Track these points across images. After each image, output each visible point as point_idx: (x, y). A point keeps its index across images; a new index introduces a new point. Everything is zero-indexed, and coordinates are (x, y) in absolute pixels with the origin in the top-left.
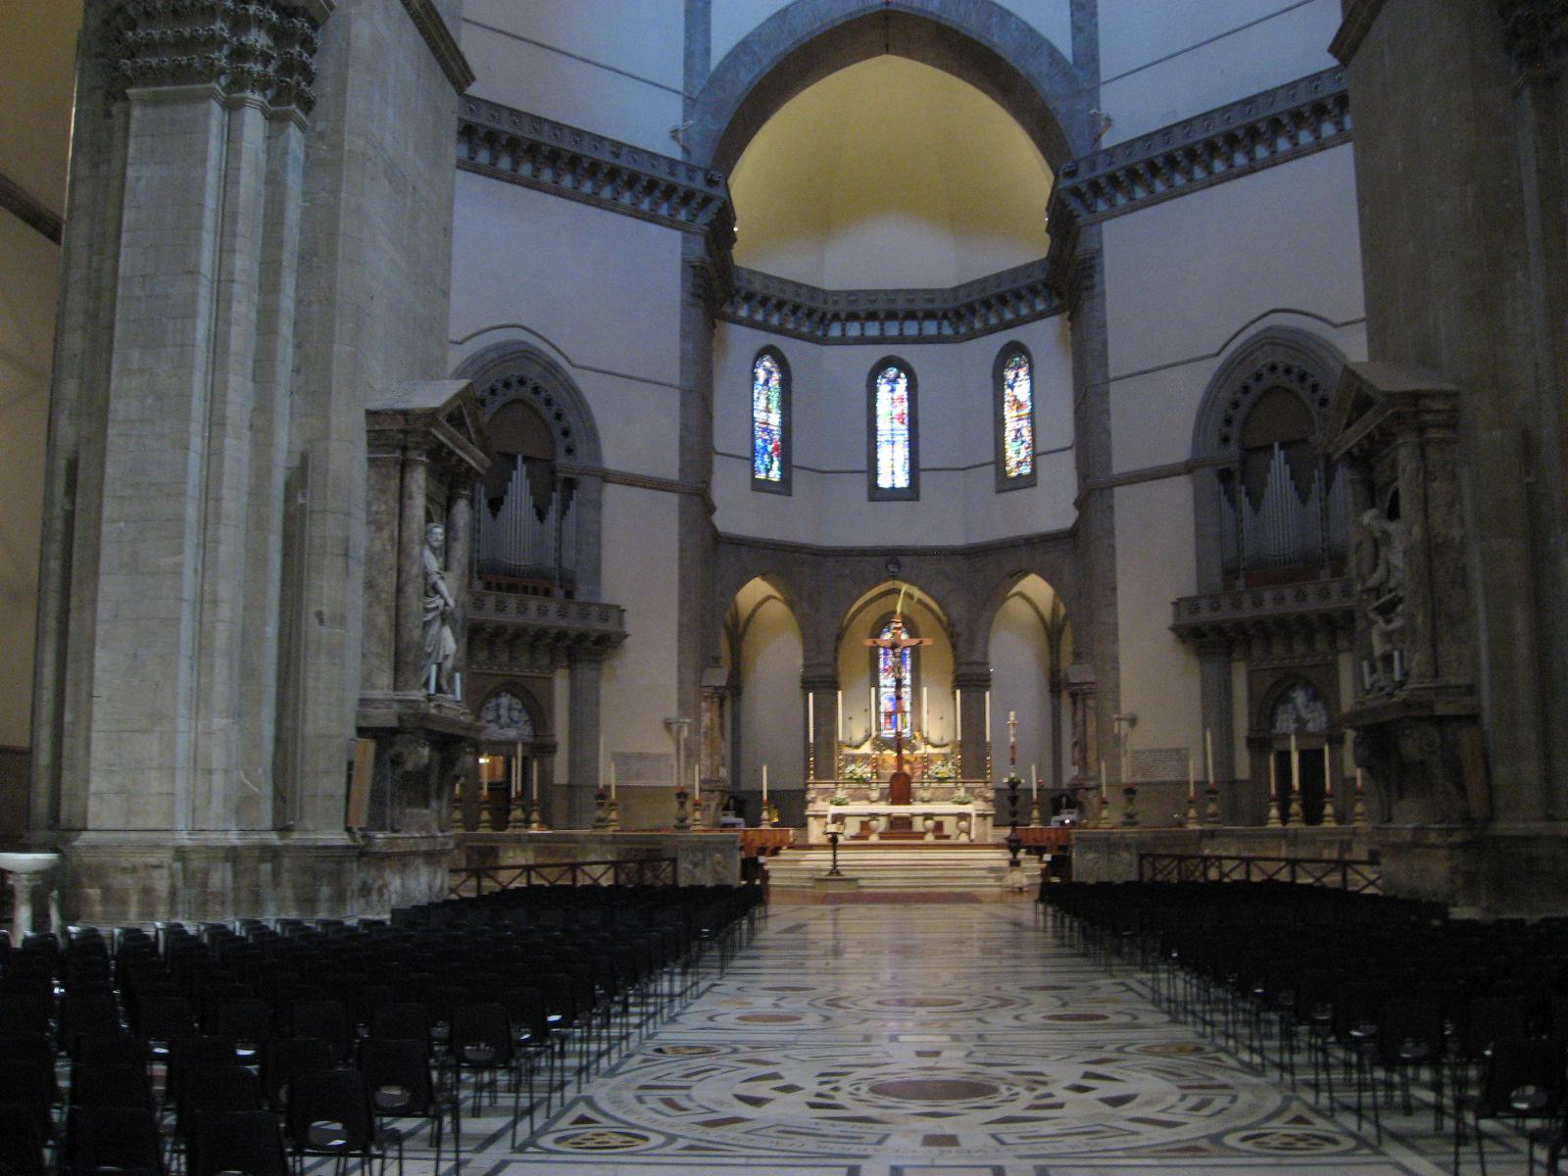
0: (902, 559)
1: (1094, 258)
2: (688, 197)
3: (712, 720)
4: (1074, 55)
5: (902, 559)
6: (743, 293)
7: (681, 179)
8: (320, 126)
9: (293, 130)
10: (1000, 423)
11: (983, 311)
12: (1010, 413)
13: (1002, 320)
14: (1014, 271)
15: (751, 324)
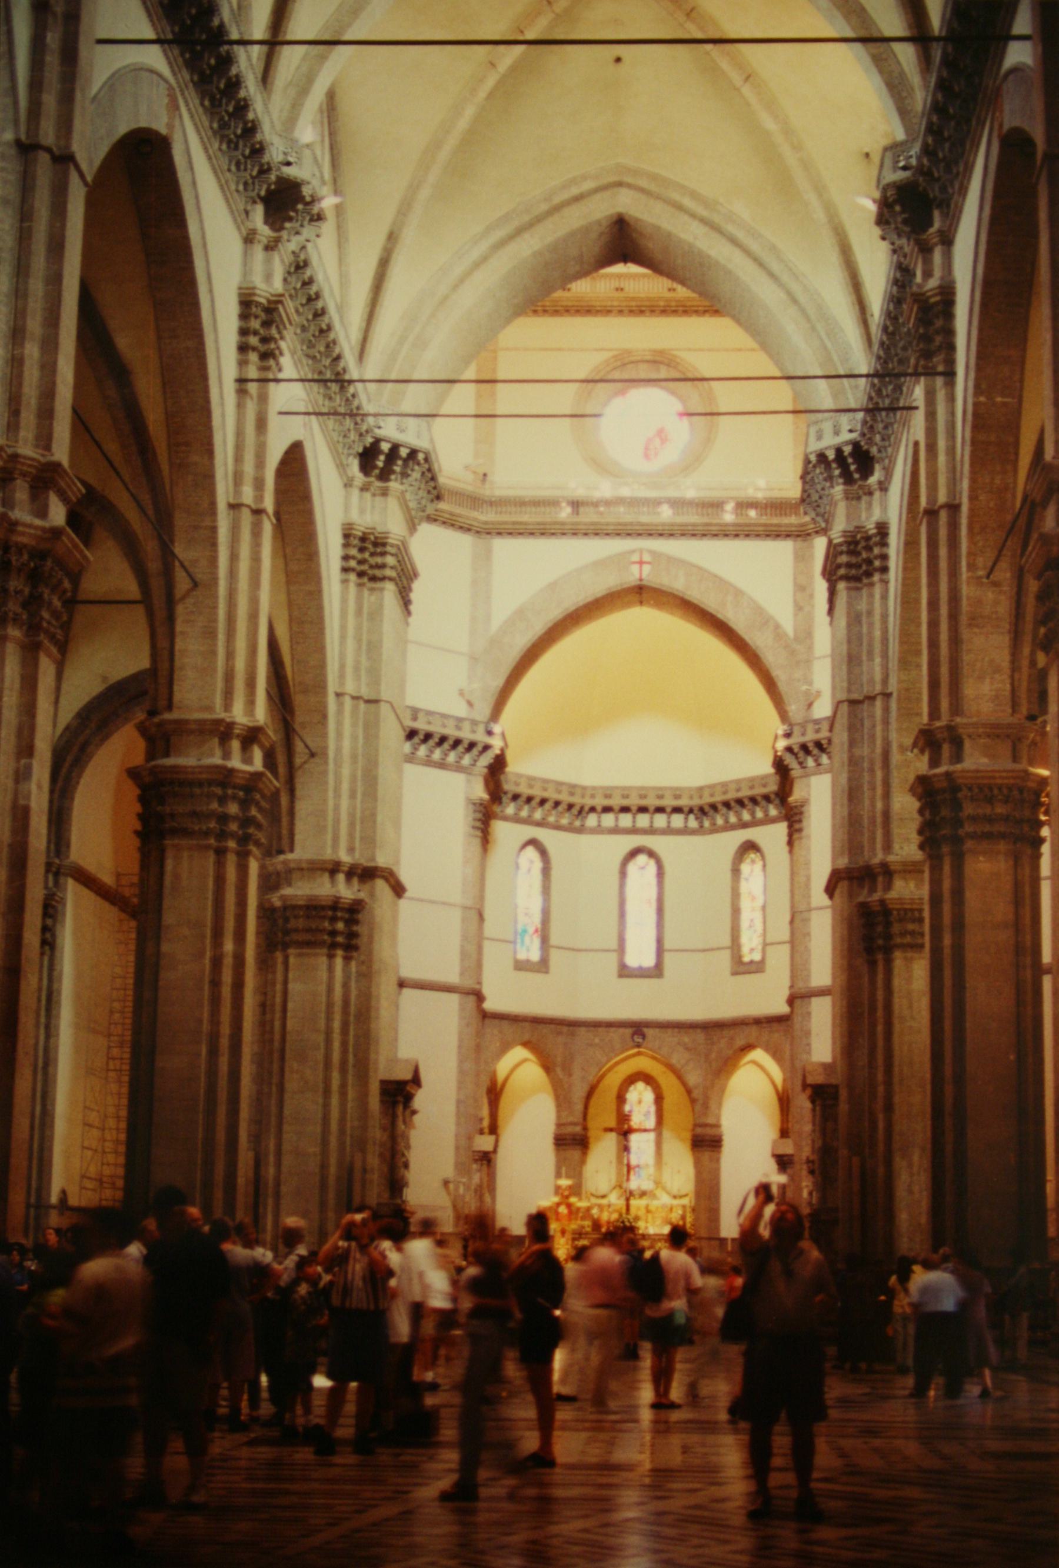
0: (645, 1030)
1: (802, 806)
2: (472, 745)
3: (481, 1179)
4: (795, 631)
5: (645, 1030)
6: (510, 796)
7: (466, 735)
8: (363, 958)
9: (353, 964)
10: (736, 911)
11: (724, 810)
12: (745, 904)
13: (740, 820)
14: (752, 781)
15: (517, 819)
